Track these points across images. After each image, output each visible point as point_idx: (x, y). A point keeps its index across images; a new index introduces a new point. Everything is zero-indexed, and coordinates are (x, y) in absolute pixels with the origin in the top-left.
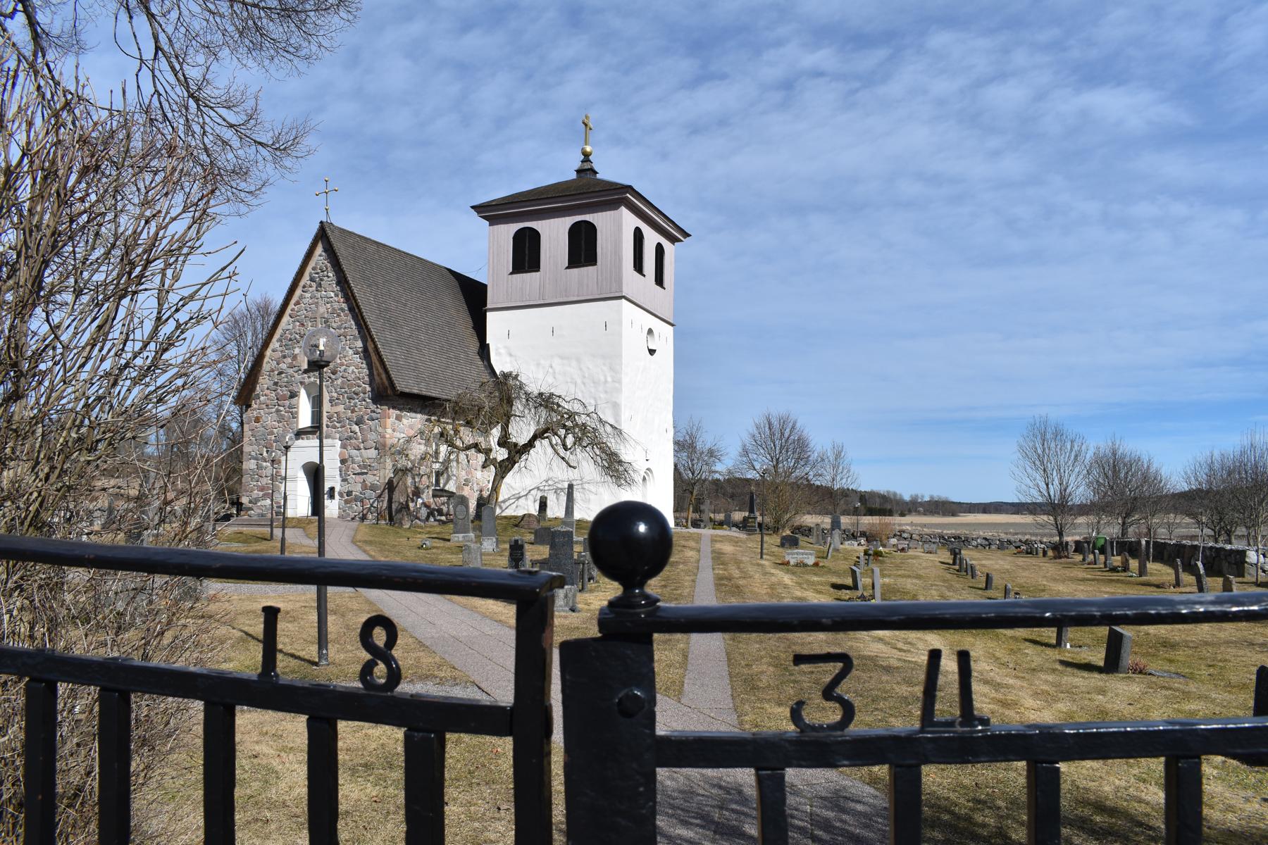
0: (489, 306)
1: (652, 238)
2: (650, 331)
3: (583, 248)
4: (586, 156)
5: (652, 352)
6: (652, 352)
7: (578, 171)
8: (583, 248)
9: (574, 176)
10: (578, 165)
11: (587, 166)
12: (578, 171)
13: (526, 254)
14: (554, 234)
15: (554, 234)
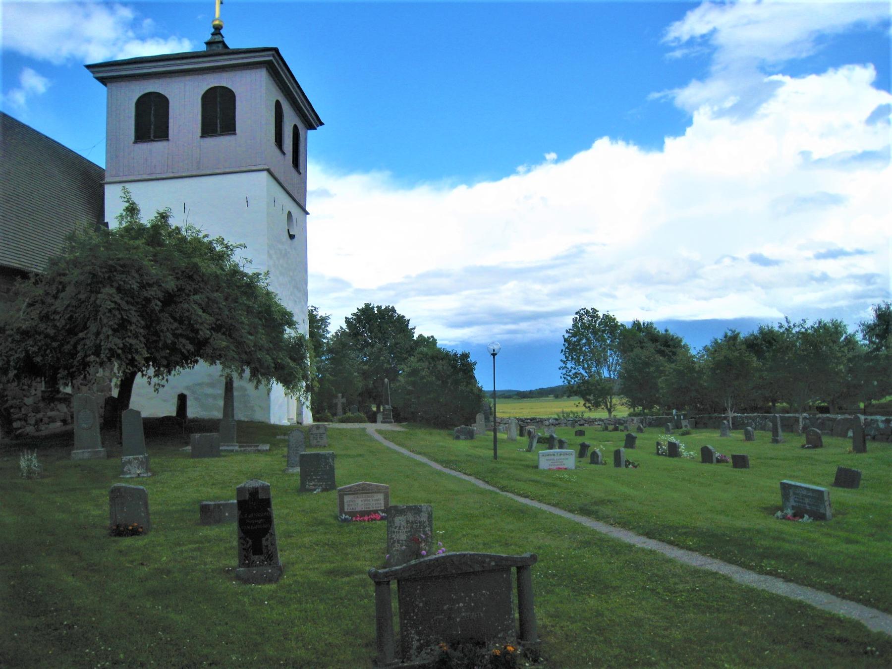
0: (107, 180)
1: (290, 119)
2: (289, 213)
3: (219, 114)
4: (218, 29)
5: (292, 237)
6: (292, 237)
7: (208, 44)
8: (219, 114)
9: (203, 48)
10: (208, 37)
11: (218, 38)
12: (208, 44)
13: (151, 121)
14: (185, 101)
15: (185, 101)
